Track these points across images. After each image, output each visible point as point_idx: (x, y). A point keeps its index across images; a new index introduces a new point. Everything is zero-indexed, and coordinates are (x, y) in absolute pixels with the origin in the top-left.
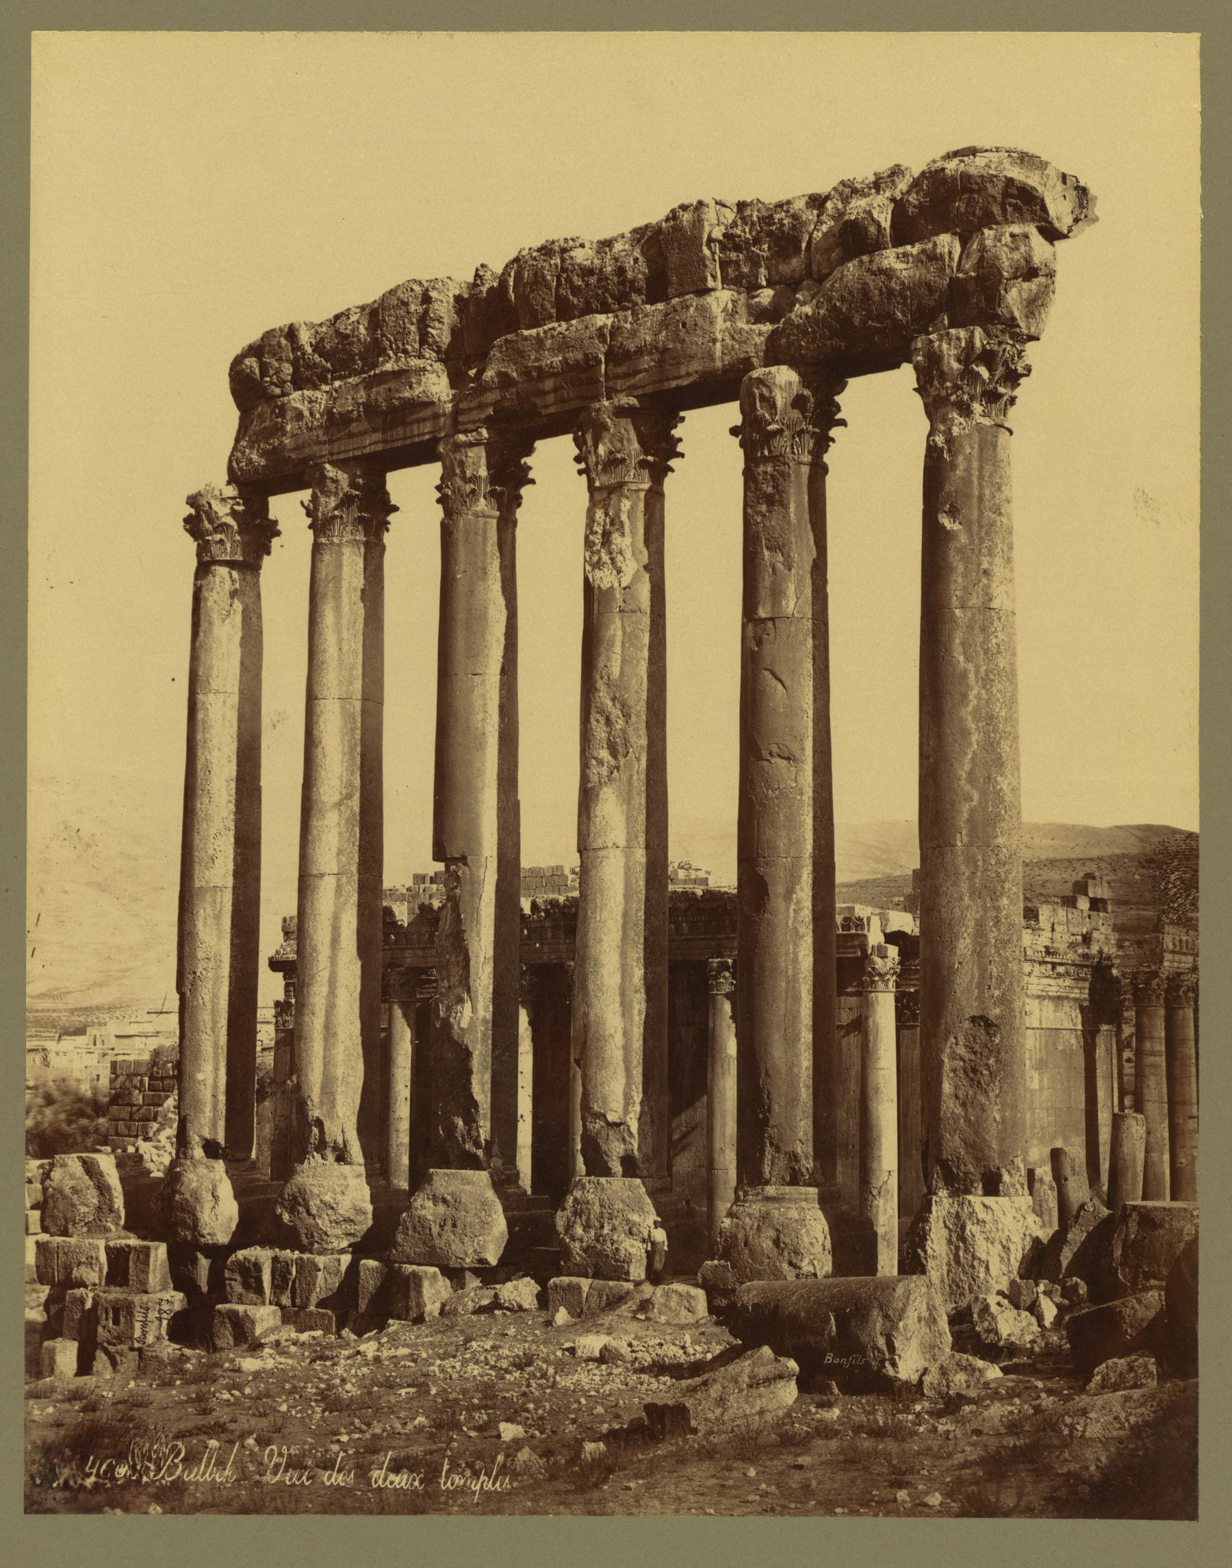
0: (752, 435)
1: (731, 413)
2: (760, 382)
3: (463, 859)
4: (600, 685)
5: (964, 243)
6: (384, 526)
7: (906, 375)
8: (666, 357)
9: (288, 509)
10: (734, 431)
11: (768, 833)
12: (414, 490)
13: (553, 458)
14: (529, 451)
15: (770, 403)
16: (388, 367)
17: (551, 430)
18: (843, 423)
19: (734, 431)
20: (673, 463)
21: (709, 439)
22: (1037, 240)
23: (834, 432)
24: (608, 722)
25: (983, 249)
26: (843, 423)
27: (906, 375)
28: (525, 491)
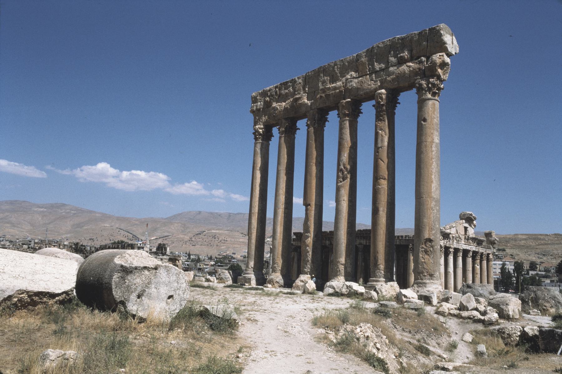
0: (378, 106)
1: (373, 102)
2: (380, 94)
3: (309, 205)
4: (341, 164)
5: (428, 58)
6: (294, 133)
7: (415, 90)
8: (358, 89)
9: (275, 131)
10: (374, 106)
11: (379, 196)
12: (302, 124)
13: (333, 116)
14: (328, 114)
15: (381, 98)
16: (297, 96)
17: (332, 109)
18: (399, 103)
19: (374, 106)
20: (360, 115)
21: (368, 108)
22: (445, 57)
23: (397, 105)
24: (343, 173)
25: (432, 59)
26: (399, 103)
27: (415, 90)
28: (327, 123)
